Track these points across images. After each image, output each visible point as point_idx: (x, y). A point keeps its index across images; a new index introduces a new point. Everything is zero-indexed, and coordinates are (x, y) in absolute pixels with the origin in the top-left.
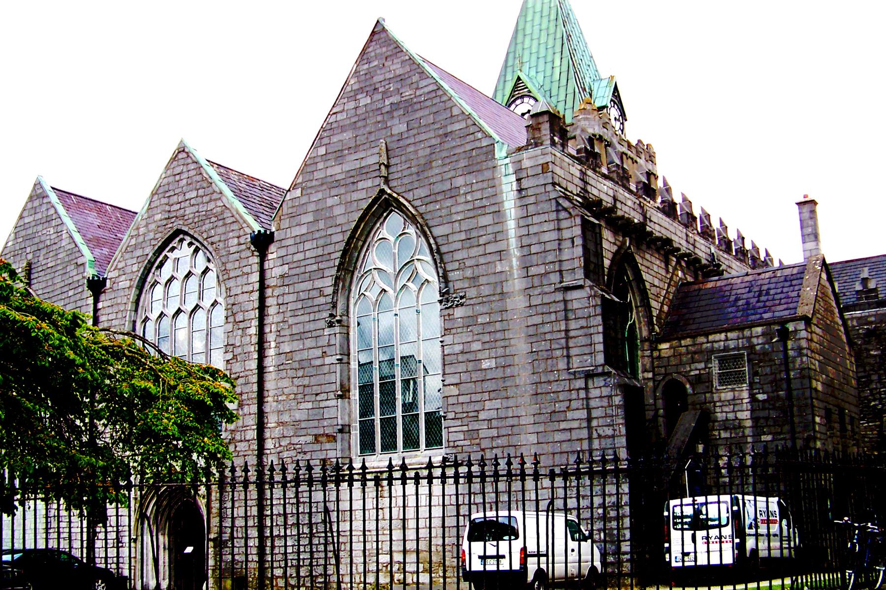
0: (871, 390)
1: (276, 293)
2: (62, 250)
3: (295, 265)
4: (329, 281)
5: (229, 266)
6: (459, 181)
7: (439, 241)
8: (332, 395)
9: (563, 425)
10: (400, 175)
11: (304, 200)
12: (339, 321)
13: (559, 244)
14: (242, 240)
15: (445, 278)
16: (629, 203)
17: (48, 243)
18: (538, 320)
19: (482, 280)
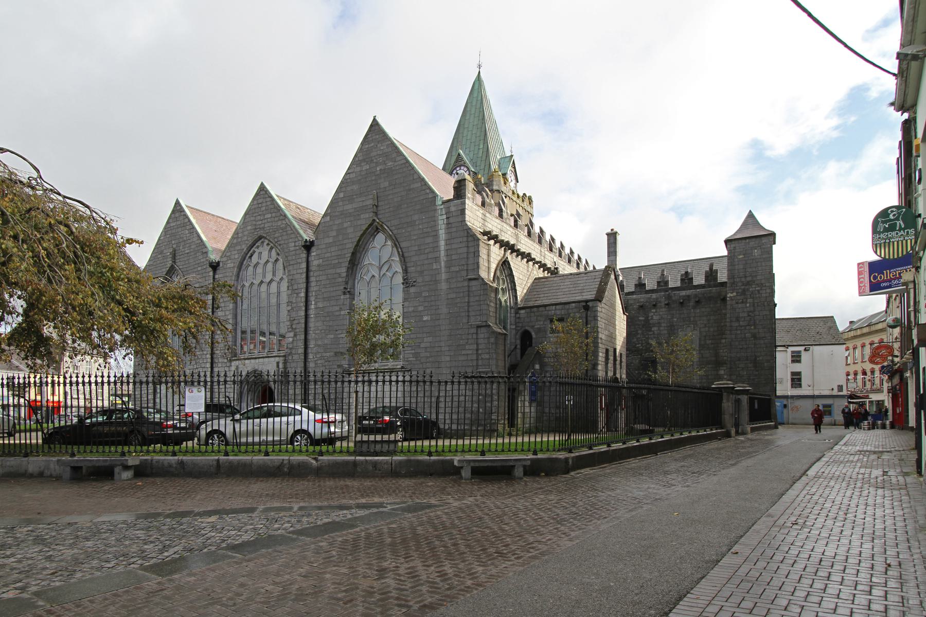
1: (315, 274)
2: (193, 243)
3: (326, 259)
4: (344, 270)
5: (290, 258)
6: (416, 217)
7: (404, 250)
8: (344, 332)
9: (463, 352)
10: (384, 212)
11: (331, 223)
12: (349, 292)
13: (467, 255)
14: (297, 244)
15: (405, 271)
16: (509, 233)
17: (185, 239)
18: (453, 296)
19: (426, 273)
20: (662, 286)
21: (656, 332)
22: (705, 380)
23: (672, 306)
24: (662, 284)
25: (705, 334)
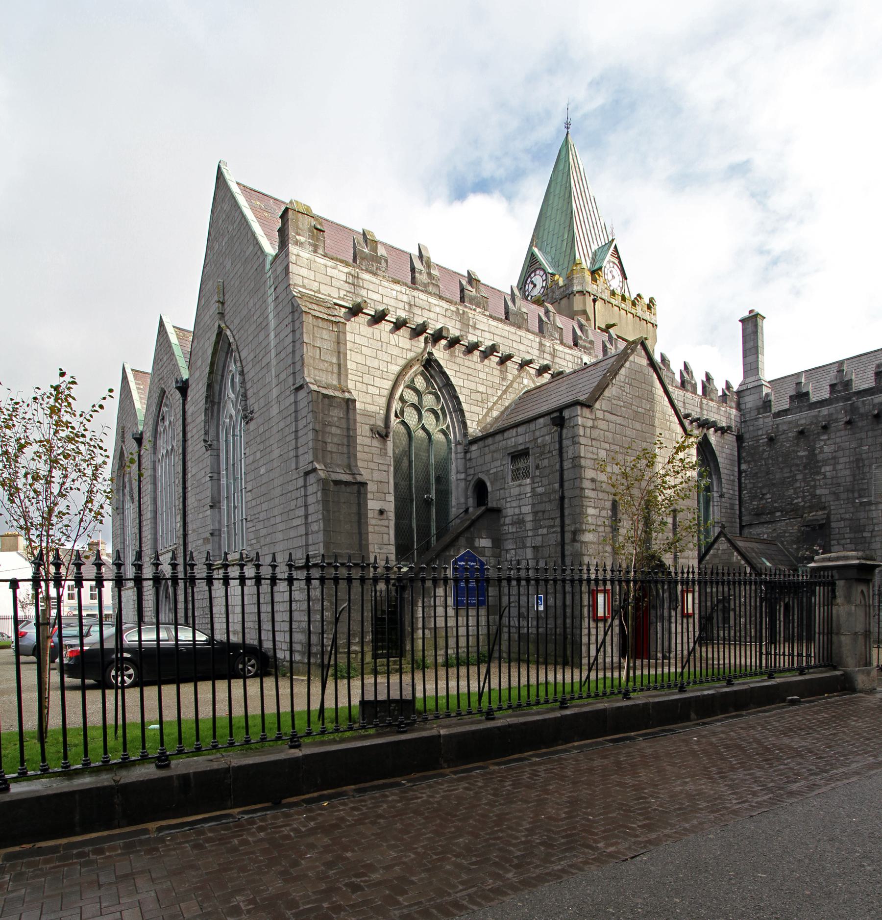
20: (840, 392)
21: (828, 475)
23: (860, 424)
24: (839, 388)
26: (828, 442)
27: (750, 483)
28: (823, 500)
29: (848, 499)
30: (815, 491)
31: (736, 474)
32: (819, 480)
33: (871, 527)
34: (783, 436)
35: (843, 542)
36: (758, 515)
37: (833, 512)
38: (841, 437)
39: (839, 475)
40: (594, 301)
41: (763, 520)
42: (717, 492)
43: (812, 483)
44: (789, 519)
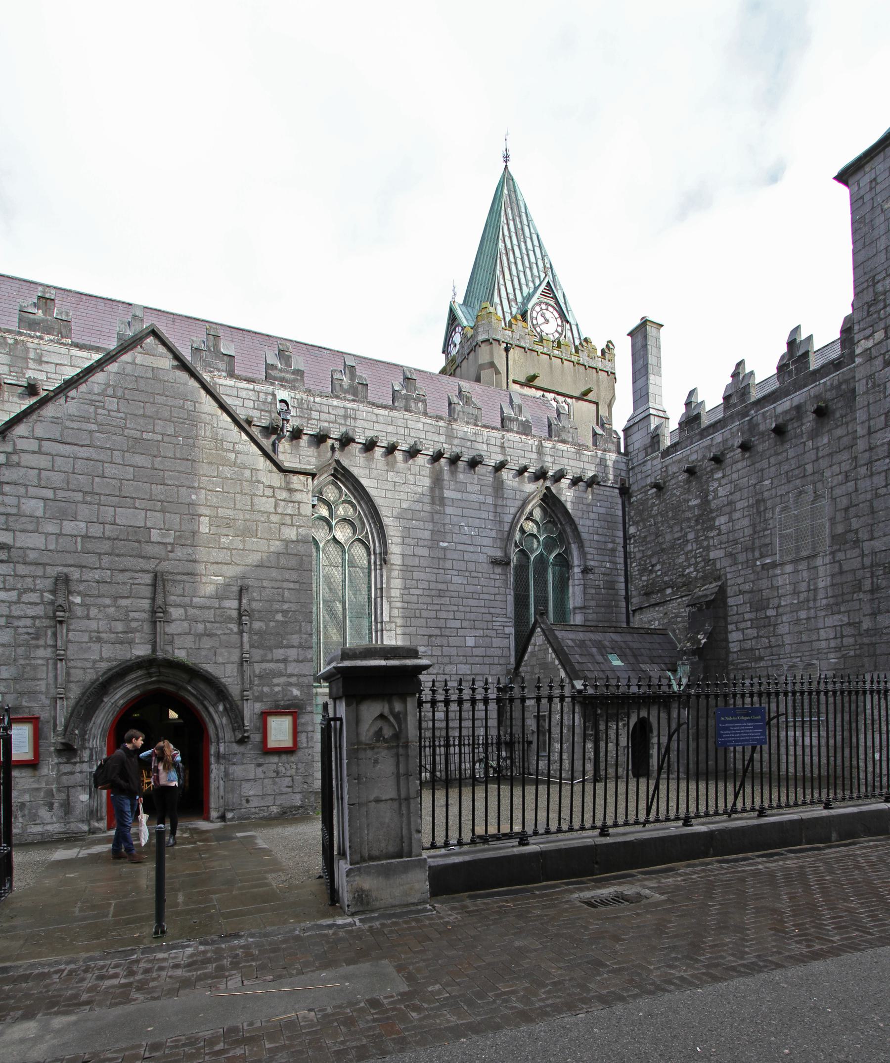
0: (686, 554)
20: (735, 405)
22: (851, 640)
23: (760, 448)
24: (734, 400)
25: (845, 502)
26: (723, 482)
27: (640, 551)
28: (718, 566)
29: (748, 561)
30: (708, 555)
31: (621, 541)
32: (713, 537)
33: (776, 601)
34: (673, 482)
35: (742, 625)
36: (647, 594)
37: (729, 583)
38: (738, 471)
39: (737, 527)
40: (507, 350)
41: (653, 601)
42: (579, 566)
43: (705, 543)
44: (681, 597)
